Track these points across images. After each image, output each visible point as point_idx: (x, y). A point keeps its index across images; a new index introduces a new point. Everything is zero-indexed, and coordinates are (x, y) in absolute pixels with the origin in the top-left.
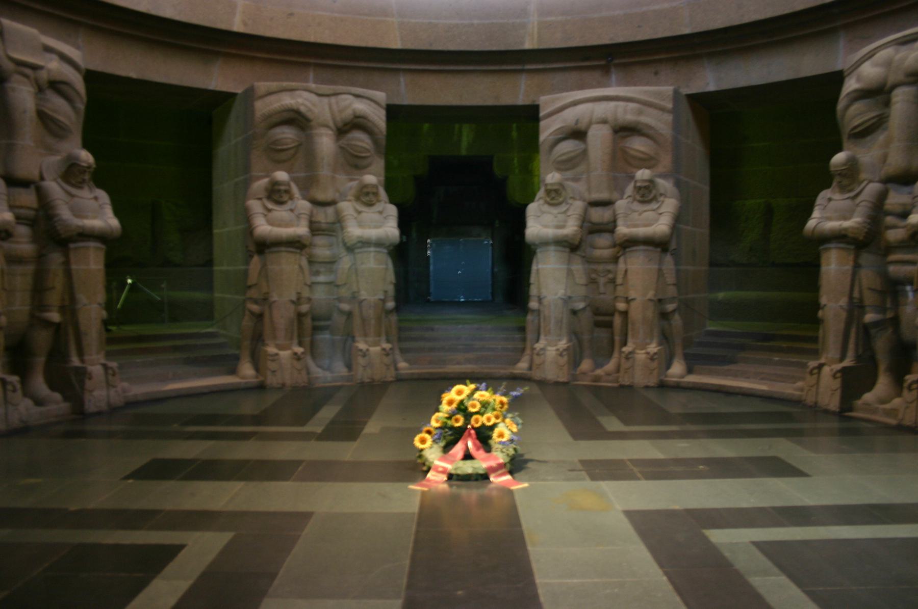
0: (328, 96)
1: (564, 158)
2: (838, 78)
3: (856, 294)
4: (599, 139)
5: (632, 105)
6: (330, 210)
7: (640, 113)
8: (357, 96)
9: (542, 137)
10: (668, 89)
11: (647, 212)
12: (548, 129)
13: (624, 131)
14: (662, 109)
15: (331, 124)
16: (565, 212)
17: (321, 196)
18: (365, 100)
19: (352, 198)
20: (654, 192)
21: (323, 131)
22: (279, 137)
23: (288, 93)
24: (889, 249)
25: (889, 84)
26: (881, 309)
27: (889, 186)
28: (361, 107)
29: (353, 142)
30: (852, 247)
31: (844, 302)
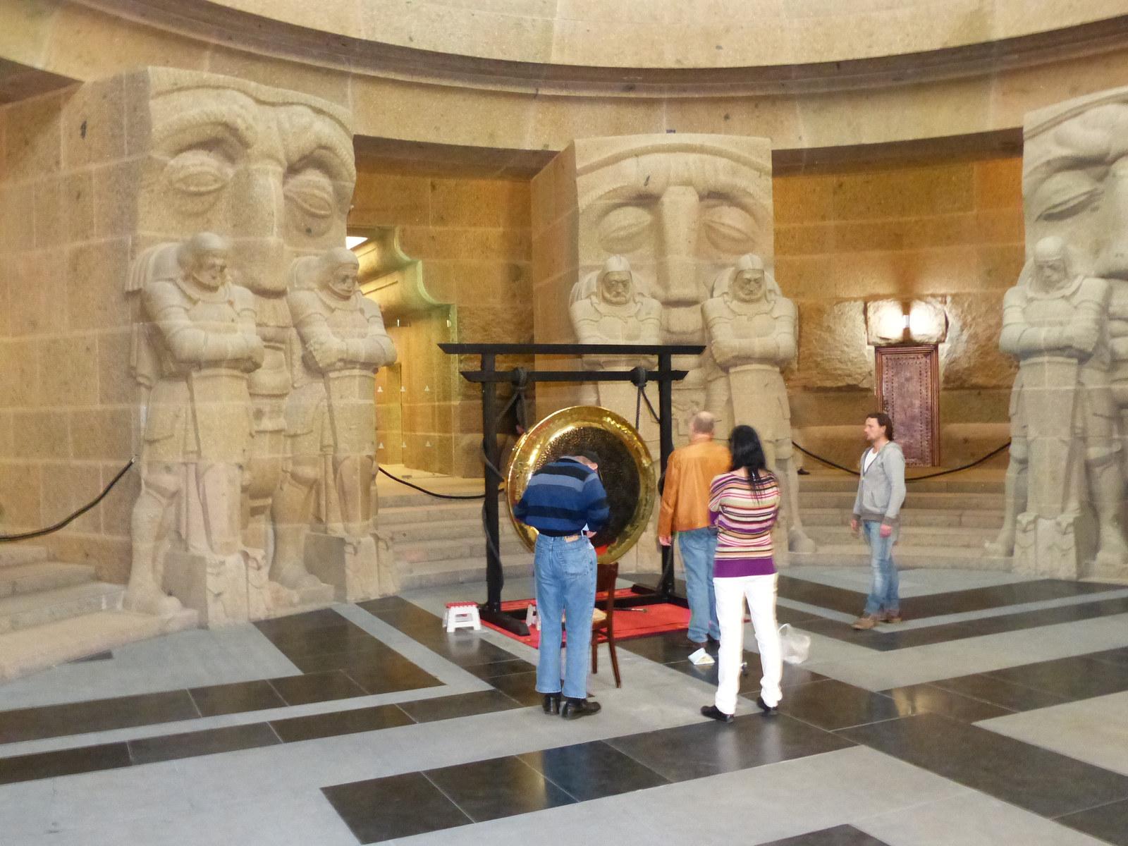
0: (273, 104)
1: (622, 233)
2: (1009, 144)
3: (1079, 424)
4: (680, 208)
5: (722, 162)
6: (281, 304)
7: (735, 173)
8: (319, 111)
9: (583, 202)
11: (1052, 305)
12: (592, 191)
13: (715, 196)
14: (759, 170)
15: (282, 156)
17: (269, 282)
19: (314, 285)
20: (763, 287)
23: (213, 93)
25: (1112, 154)
26: (1110, 442)
27: (1113, 282)
28: (323, 129)
30: (1075, 361)
31: (1065, 434)
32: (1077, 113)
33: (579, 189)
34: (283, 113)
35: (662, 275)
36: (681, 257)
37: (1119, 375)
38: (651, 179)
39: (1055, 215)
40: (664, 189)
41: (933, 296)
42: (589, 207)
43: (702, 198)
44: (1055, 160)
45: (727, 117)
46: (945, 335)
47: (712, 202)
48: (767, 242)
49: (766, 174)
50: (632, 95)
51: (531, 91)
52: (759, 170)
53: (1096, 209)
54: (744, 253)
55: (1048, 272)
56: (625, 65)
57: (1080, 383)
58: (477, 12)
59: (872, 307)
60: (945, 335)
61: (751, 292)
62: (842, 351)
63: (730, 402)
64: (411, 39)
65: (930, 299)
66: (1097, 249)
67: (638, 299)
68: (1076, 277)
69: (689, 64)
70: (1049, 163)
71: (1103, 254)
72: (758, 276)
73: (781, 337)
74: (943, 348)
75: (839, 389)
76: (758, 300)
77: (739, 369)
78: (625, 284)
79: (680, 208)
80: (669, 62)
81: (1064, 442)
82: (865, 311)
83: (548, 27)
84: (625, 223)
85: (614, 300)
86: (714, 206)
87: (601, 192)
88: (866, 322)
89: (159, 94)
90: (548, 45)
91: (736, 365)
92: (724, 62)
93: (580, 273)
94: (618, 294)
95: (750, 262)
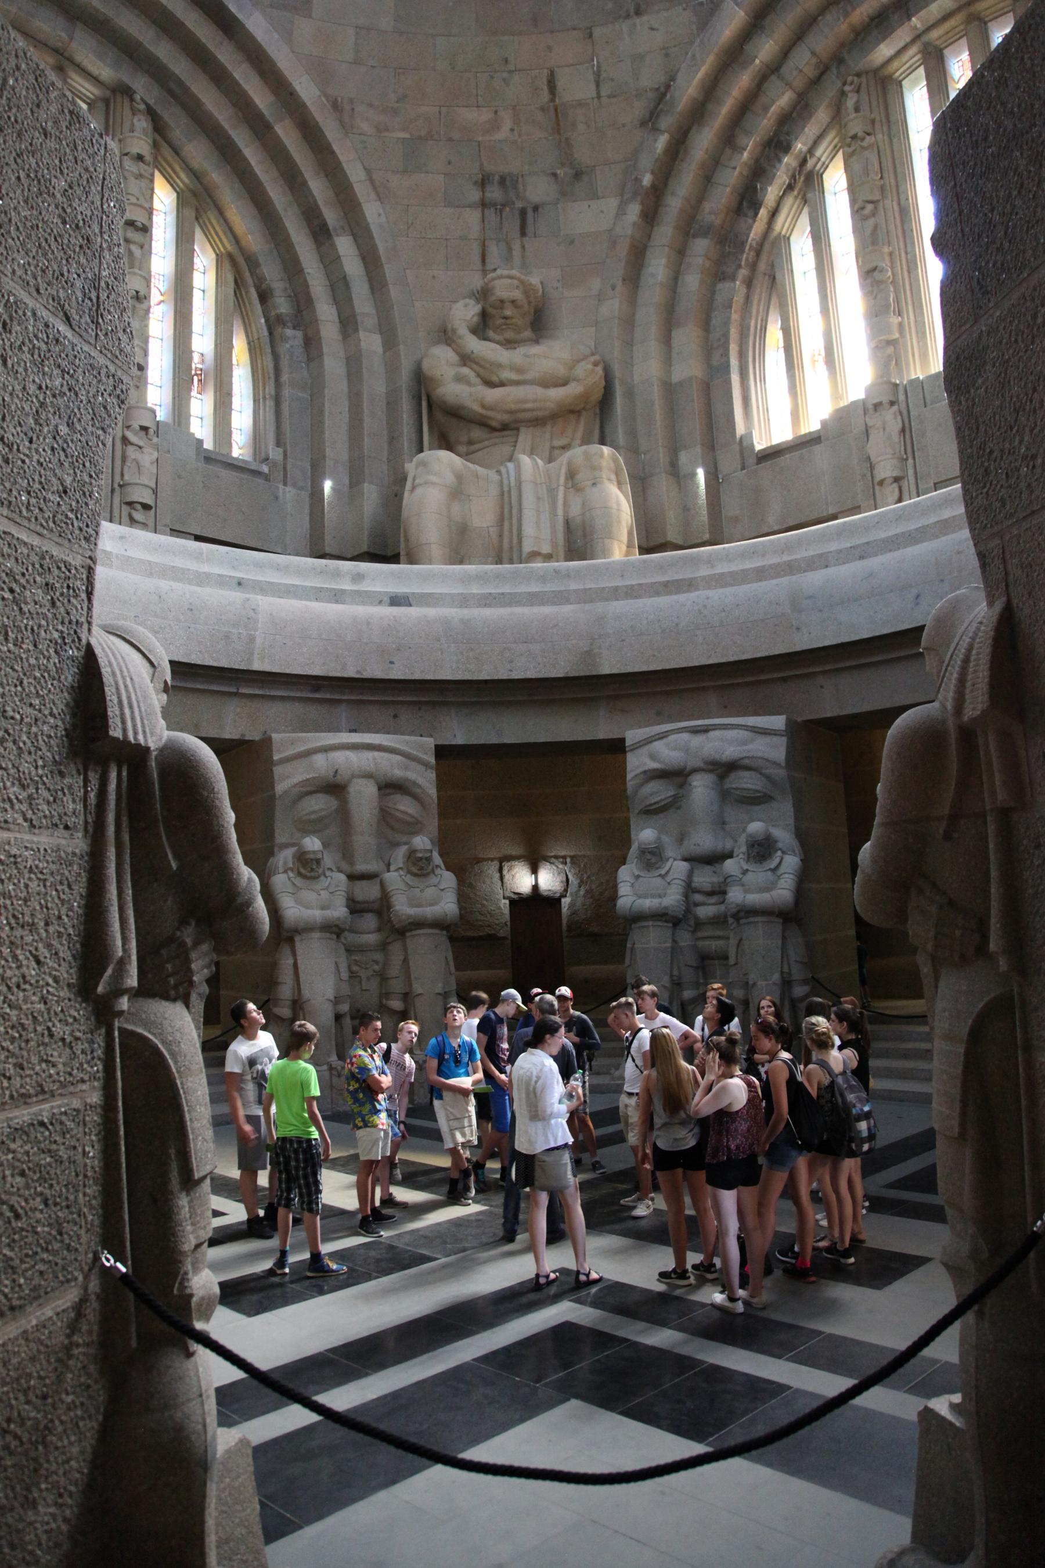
1: (313, 816)
3: (676, 973)
4: (364, 797)
7: (406, 768)
9: (280, 788)
10: (430, 742)
13: (390, 787)
14: (425, 764)
24: (699, 924)
25: (688, 768)
32: (662, 736)
33: (276, 777)
35: (347, 853)
36: (364, 839)
37: (700, 934)
38: (339, 772)
39: (651, 812)
40: (349, 781)
41: (556, 857)
42: (286, 793)
43: (380, 789)
44: (649, 770)
45: (395, 716)
46: (566, 890)
47: (388, 791)
48: (433, 824)
49: (431, 768)
50: (317, 696)
51: (233, 690)
52: (425, 764)
53: (679, 808)
54: (415, 833)
55: (649, 856)
56: (314, 673)
57: (674, 941)
58: (192, 625)
59: (506, 866)
60: (566, 890)
61: (422, 868)
62: (483, 905)
63: (406, 960)
65: (553, 860)
66: (681, 838)
67: (328, 873)
68: (668, 860)
69: (367, 675)
70: (645, 772)
71: (686, 842)
72: (428, 855)
73: (447, 905)
74: (566, 902)
75: (481, 938)
76: (427, 875)
77: (414, 933)
78: (318, 862)
79: (364, 797)
80: (351, 673)
81: (665, 987)
82: (501, 870)
83: (252, 639)
84: (317, 808)
85: (308, 874)
86: (389, 794)
87: (296, 781)
88: (502, 878)
90: (252, 654)
91: (411, 930)
92: (396, 674)
93: (276, 849)
94: (312, 870)
95: (421, 842)
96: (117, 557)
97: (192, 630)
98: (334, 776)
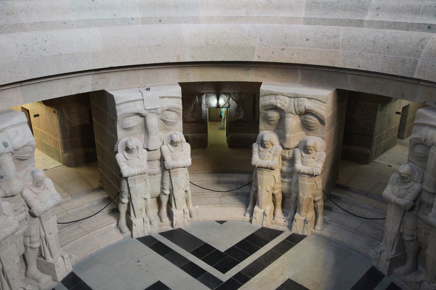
6: (291, 151)
16: (407, 189)
17: (286, 146)
18: (313, 100)
21: (290, 115)
22: (270, 115)
23: (274, 96)
29: (307, 120)
34: (296, 99)
38: (427, 141)
64: (359, 67)
83: (416, 62)
89: (262, 96)
90: (414, 70)
96: (367, 21)
97: (386, 58)
98: (425, 141)
